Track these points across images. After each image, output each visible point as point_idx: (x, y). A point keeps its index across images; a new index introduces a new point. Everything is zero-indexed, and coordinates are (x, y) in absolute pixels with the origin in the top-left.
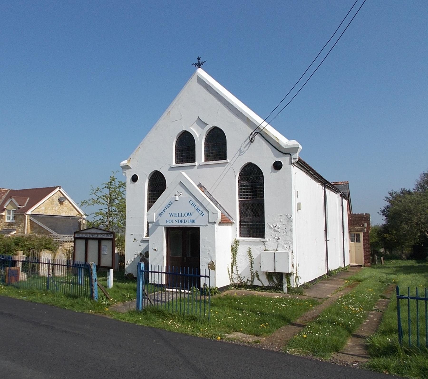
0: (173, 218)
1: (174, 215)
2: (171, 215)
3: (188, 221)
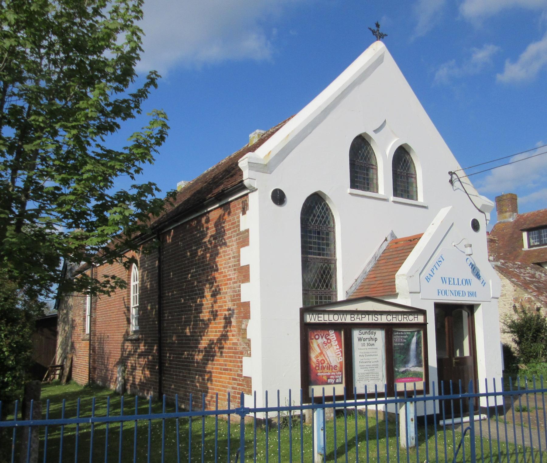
0: (446, 287)
2: (443, 280)
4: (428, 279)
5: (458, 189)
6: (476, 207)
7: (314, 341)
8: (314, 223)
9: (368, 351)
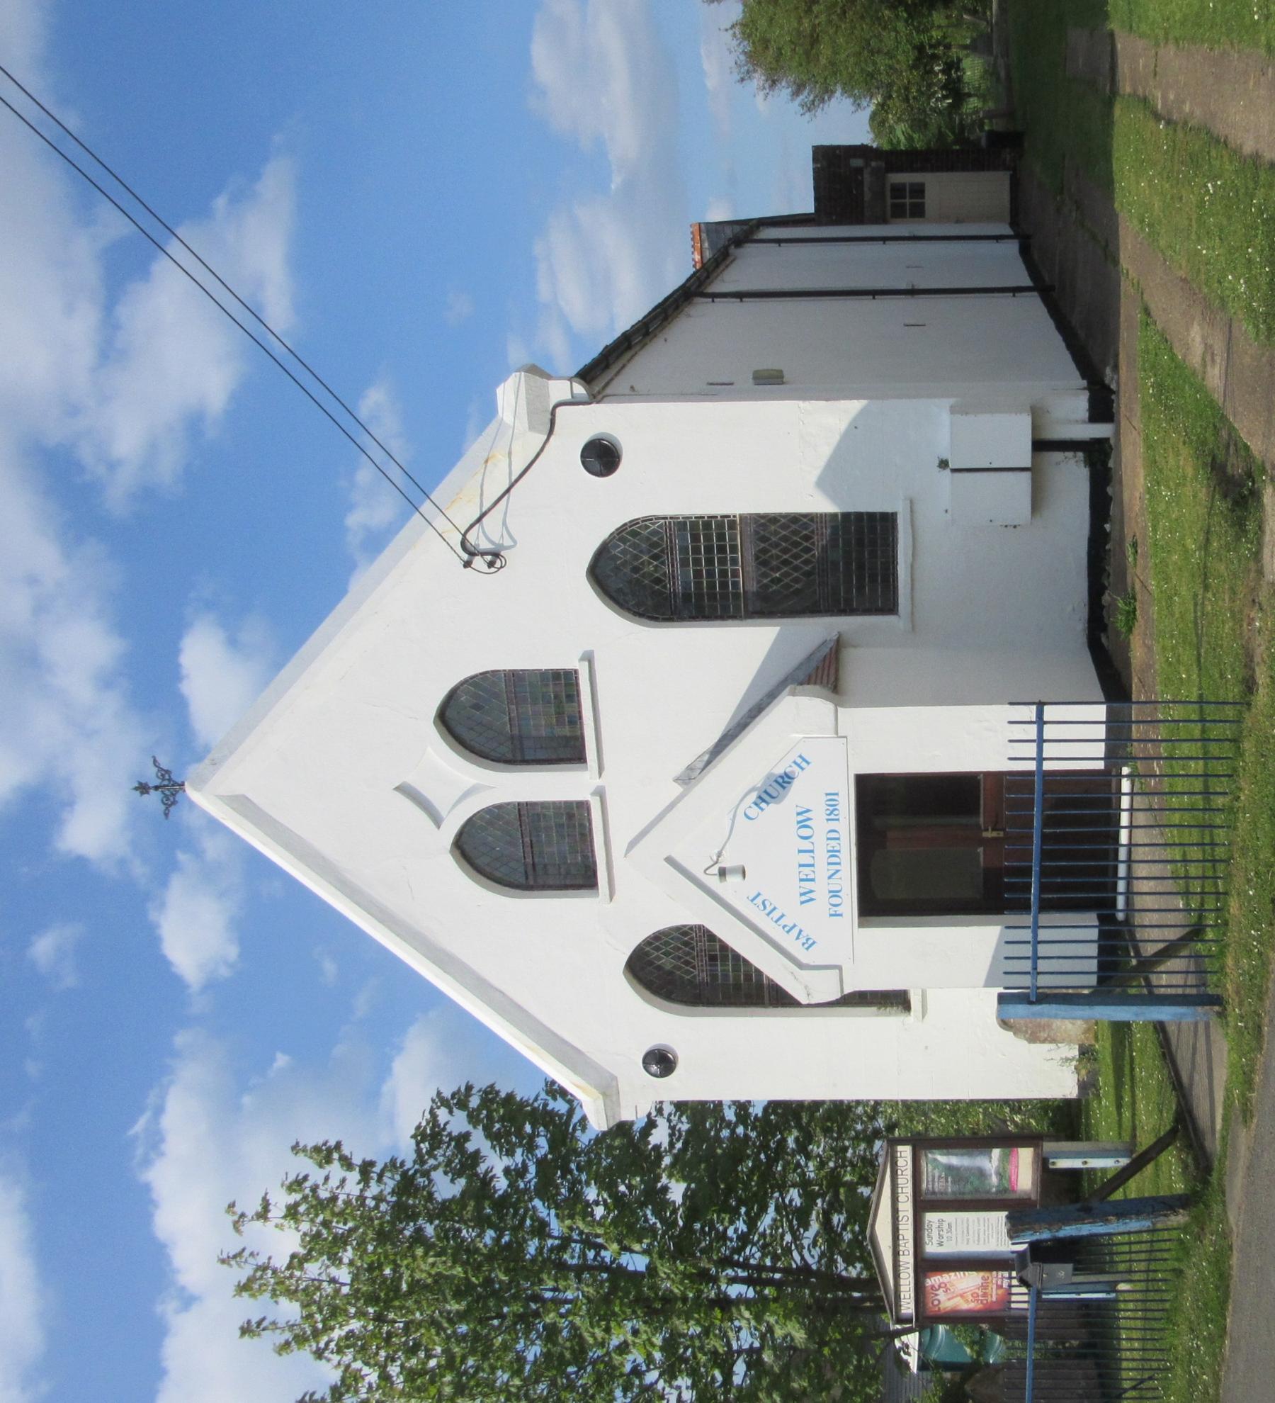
0: (821, 888)
1: (809, 885)
2: (807, 898)
3: (833, 825)
4: (809, 944)
5: (504, 523)
6: (542, 450)
7: (942, 1306)
8: (694, 967)
9: (959, 1232)
